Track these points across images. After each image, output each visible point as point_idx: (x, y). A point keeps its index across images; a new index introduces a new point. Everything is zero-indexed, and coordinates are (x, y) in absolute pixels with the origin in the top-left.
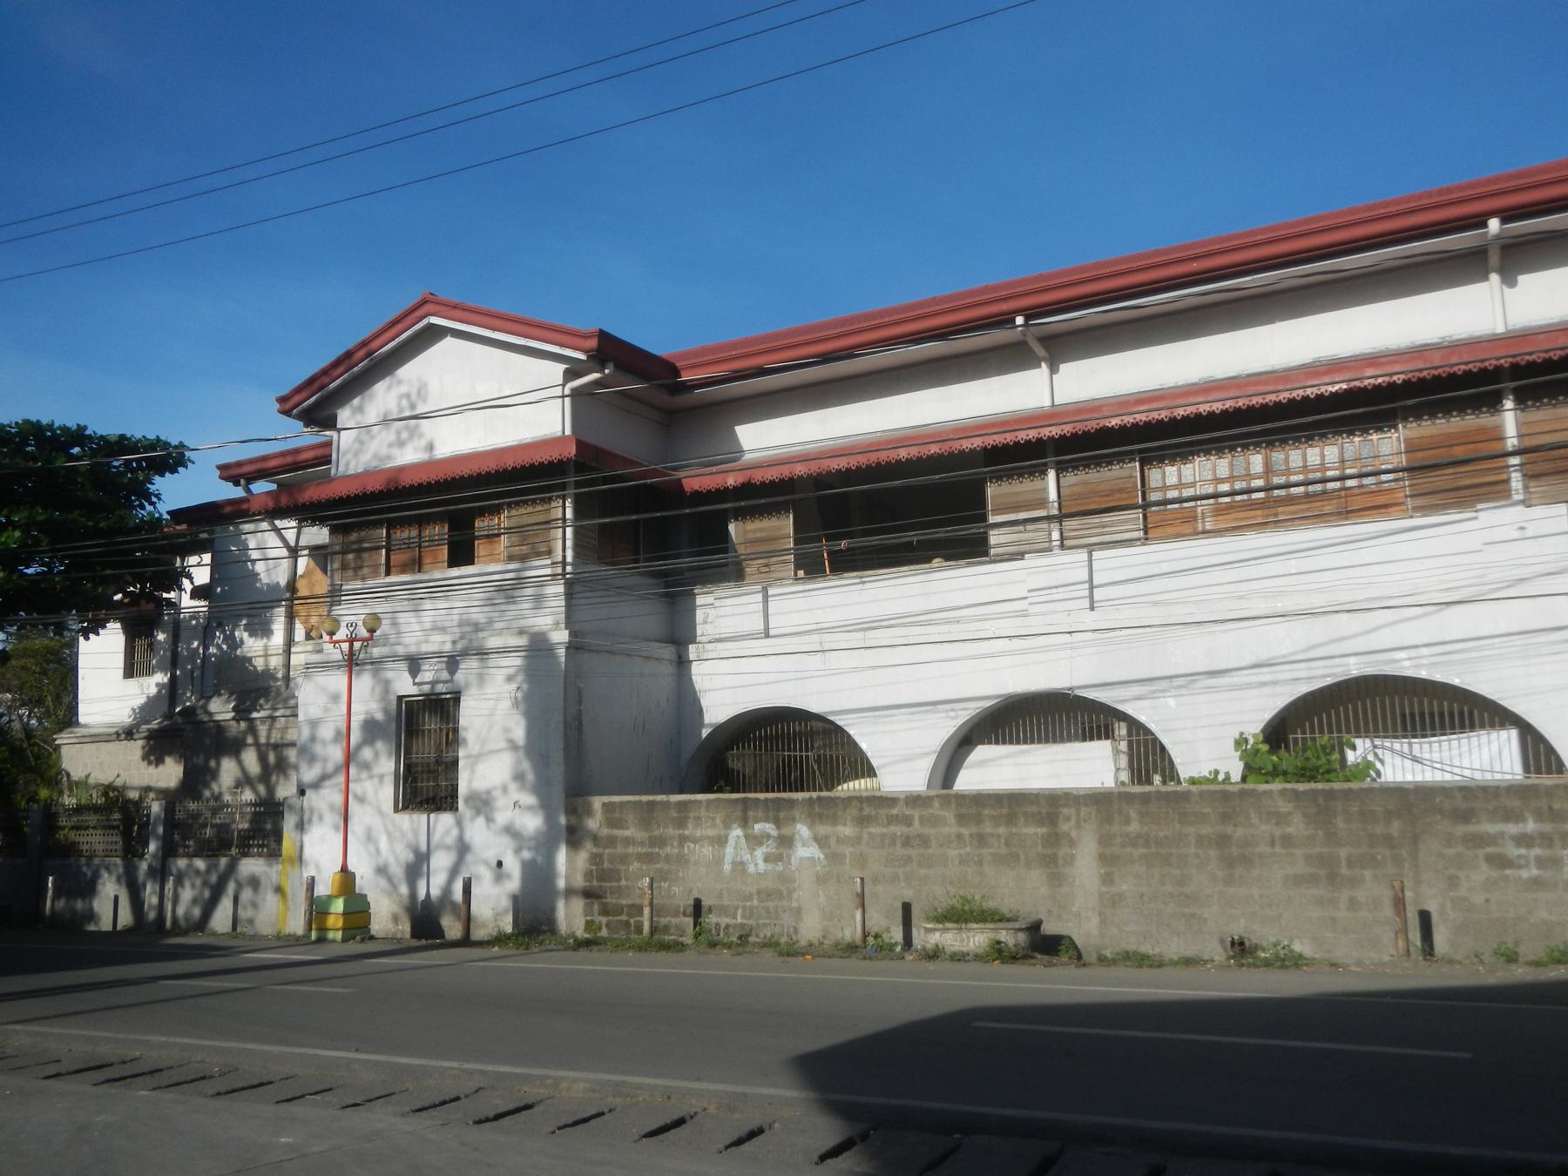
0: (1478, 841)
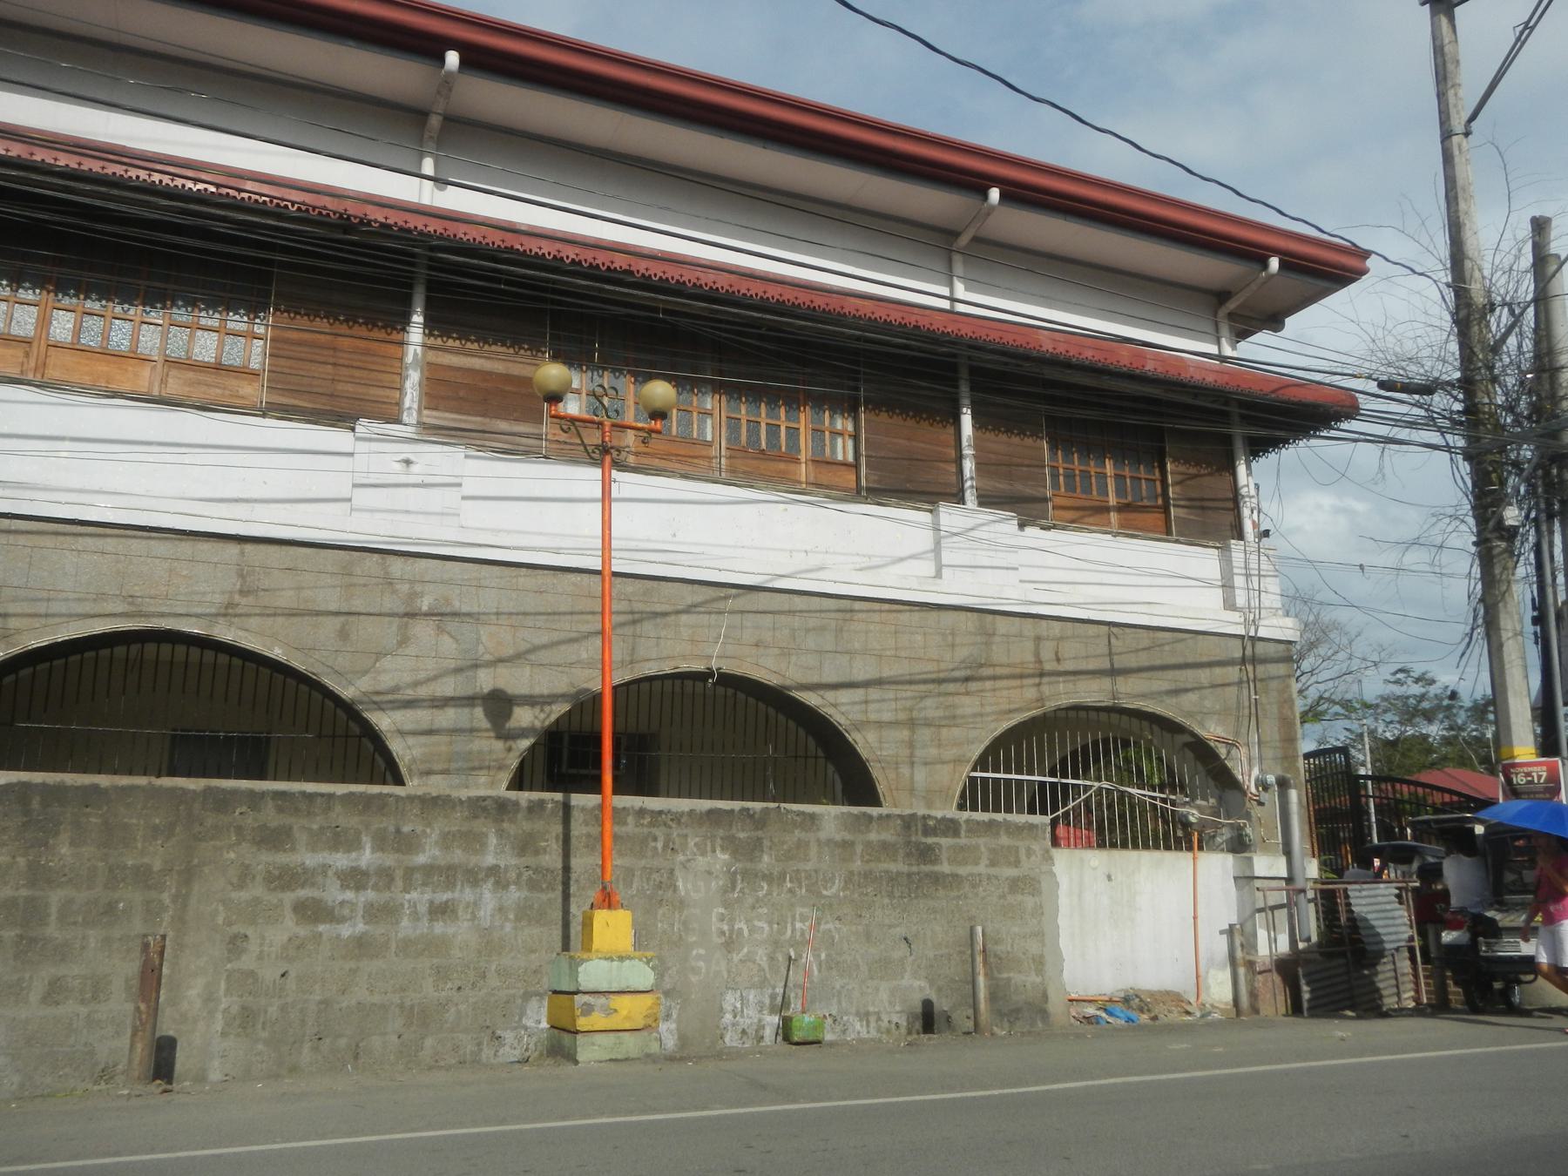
0: (285, 879)
